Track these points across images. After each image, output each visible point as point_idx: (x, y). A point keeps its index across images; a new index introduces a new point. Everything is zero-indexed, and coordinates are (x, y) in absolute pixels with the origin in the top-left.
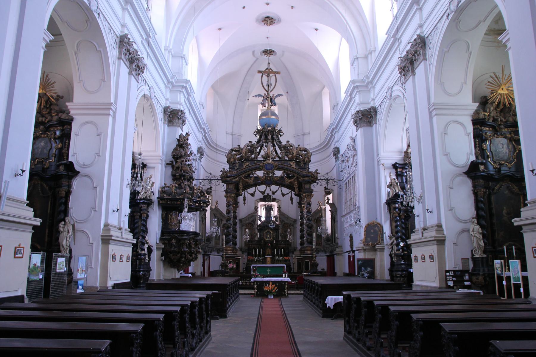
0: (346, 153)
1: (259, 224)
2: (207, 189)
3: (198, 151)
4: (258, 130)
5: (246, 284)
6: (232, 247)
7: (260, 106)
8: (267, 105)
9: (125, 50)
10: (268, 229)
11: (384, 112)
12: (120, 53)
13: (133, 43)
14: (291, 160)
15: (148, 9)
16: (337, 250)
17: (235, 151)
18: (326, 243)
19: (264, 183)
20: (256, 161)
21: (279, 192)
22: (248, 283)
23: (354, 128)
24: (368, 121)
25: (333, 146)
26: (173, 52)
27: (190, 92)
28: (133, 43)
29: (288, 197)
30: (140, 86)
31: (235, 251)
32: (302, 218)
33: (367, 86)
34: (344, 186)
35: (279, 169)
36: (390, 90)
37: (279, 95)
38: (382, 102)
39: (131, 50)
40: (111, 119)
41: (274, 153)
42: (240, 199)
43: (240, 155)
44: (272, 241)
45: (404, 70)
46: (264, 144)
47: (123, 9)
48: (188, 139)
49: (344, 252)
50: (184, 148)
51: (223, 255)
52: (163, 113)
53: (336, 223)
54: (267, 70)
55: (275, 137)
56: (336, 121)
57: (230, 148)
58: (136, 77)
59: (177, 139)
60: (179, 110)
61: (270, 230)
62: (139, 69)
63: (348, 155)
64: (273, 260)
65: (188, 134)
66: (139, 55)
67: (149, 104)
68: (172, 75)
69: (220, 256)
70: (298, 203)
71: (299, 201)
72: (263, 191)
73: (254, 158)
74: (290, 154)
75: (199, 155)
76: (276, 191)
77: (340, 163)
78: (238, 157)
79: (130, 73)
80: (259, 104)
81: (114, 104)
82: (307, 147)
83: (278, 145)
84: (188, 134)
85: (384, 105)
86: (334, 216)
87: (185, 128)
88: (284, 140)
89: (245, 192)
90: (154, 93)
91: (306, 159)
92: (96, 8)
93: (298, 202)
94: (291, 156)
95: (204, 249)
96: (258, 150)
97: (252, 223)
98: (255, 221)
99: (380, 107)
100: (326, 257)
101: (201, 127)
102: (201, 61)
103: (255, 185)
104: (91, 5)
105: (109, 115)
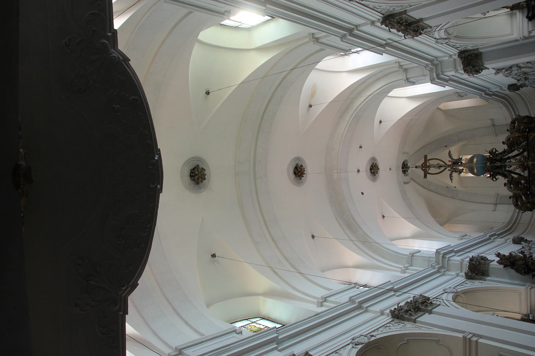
0: (515, 77)
3: (518, 244)
4: (490, 177)
7: (462, 174)
9: (406, 314)
11: (461, 42)
12: (409, 320)
13: (399, 305)
14: (526, 139)
15: (365, 286)
17: (517, 202)
20: (529, 178)
23: (484, 72)
24: (475, 59)
25: (507, 92)
26: (407, 265)
27: (447, 251)
28: (399, 305)
30: (443, 303)
33: (436, 65)
36: (439, 41)
38: (453, 46)
39: (405, 308)
40: (481, 340)
41: (518, 158)
43: (521, 196)
45: (417, 31)
46: (507, 169)
47: (366, 311)
48: (504, 256)
50: (515, 260)
52: (473, 281)
55: (498, 158)
57: (512, 207)
58: (434, 306)
59: (504, 267)
60: (469, 263)
62: (425, 302)
63: (518, 74)
65: (498, 255)
66: (411, 300)
67: (463, 295)
68: (431, 268)
73: (526, 180)
74: (520, 140)
75: (523, 243)
78: (524, 198)
79: (430, 312)
80: (460, 176)
81: (464, 335)
82: (509, 121)
83: (508, 154)
84: (498, 255)
85: (456, 44)
87: (490, 257)
88: (501, 148)
90: (451, 289)
91: (525, 121)
92: (366, 338)
94: (521, 139)
96: (516, 176)
99: (458, 48)
102: (415, 236)
104: (363, 342)
105: (477, 341)
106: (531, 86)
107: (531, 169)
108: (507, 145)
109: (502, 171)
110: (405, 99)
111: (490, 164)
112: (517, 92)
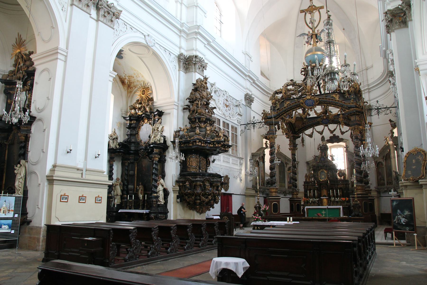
8: (312, 43)
10: (322, 169)
19: (320, 122)
61: (324, 170)
64: (329, 201)
72: (321, 130)
76: (335, 130)
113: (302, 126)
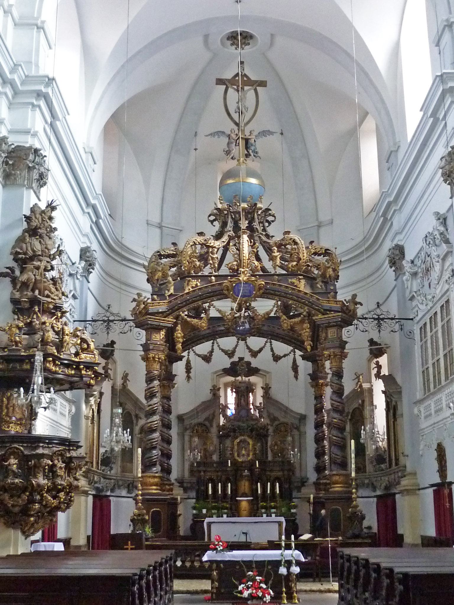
1: (221, 424)
2: (104, 346)
4: (217, 209)
5: (192, 566)
6: (160, 477)
10: (243, 435)
16: (405, 482)
18: (374, 466)
21: (267, 351)
22: (197, 561)
25: (388, 245)
29: (287, 362)
31: (167, 487)
32: (318, 410)
34: (417, 332)
35: (266, 295)
37: (264, 133)
42: (179, 368)
44: (252, 464)
49: (420, 487)
51: (137, 495)
53: (399, 420)
54: (237, 78)
55: (256, 225)
56: (396, 185)
61: (246, 438)
69: (131, 500)
70: (309, 377)
71: (311, 372)
77: (407, 280)
86: (394, 403)
89: (189, 353)
93: (309, 375)
95: (96, 483)
97: (207, 423)
98: (213, 418)
100: (375, 499)
101: (88, 204)
103: (213, 336)
106: (395, 286)
107: (233, 280)
108: (282, 240)
109: (230, 231)
110: (394, 37)
111: (244, 209)
112: (387, 262)
113: (190, 335)
